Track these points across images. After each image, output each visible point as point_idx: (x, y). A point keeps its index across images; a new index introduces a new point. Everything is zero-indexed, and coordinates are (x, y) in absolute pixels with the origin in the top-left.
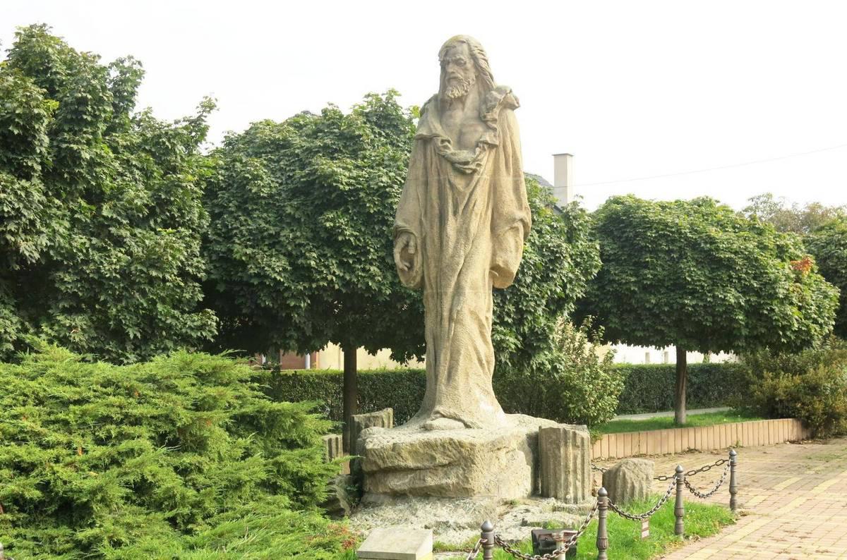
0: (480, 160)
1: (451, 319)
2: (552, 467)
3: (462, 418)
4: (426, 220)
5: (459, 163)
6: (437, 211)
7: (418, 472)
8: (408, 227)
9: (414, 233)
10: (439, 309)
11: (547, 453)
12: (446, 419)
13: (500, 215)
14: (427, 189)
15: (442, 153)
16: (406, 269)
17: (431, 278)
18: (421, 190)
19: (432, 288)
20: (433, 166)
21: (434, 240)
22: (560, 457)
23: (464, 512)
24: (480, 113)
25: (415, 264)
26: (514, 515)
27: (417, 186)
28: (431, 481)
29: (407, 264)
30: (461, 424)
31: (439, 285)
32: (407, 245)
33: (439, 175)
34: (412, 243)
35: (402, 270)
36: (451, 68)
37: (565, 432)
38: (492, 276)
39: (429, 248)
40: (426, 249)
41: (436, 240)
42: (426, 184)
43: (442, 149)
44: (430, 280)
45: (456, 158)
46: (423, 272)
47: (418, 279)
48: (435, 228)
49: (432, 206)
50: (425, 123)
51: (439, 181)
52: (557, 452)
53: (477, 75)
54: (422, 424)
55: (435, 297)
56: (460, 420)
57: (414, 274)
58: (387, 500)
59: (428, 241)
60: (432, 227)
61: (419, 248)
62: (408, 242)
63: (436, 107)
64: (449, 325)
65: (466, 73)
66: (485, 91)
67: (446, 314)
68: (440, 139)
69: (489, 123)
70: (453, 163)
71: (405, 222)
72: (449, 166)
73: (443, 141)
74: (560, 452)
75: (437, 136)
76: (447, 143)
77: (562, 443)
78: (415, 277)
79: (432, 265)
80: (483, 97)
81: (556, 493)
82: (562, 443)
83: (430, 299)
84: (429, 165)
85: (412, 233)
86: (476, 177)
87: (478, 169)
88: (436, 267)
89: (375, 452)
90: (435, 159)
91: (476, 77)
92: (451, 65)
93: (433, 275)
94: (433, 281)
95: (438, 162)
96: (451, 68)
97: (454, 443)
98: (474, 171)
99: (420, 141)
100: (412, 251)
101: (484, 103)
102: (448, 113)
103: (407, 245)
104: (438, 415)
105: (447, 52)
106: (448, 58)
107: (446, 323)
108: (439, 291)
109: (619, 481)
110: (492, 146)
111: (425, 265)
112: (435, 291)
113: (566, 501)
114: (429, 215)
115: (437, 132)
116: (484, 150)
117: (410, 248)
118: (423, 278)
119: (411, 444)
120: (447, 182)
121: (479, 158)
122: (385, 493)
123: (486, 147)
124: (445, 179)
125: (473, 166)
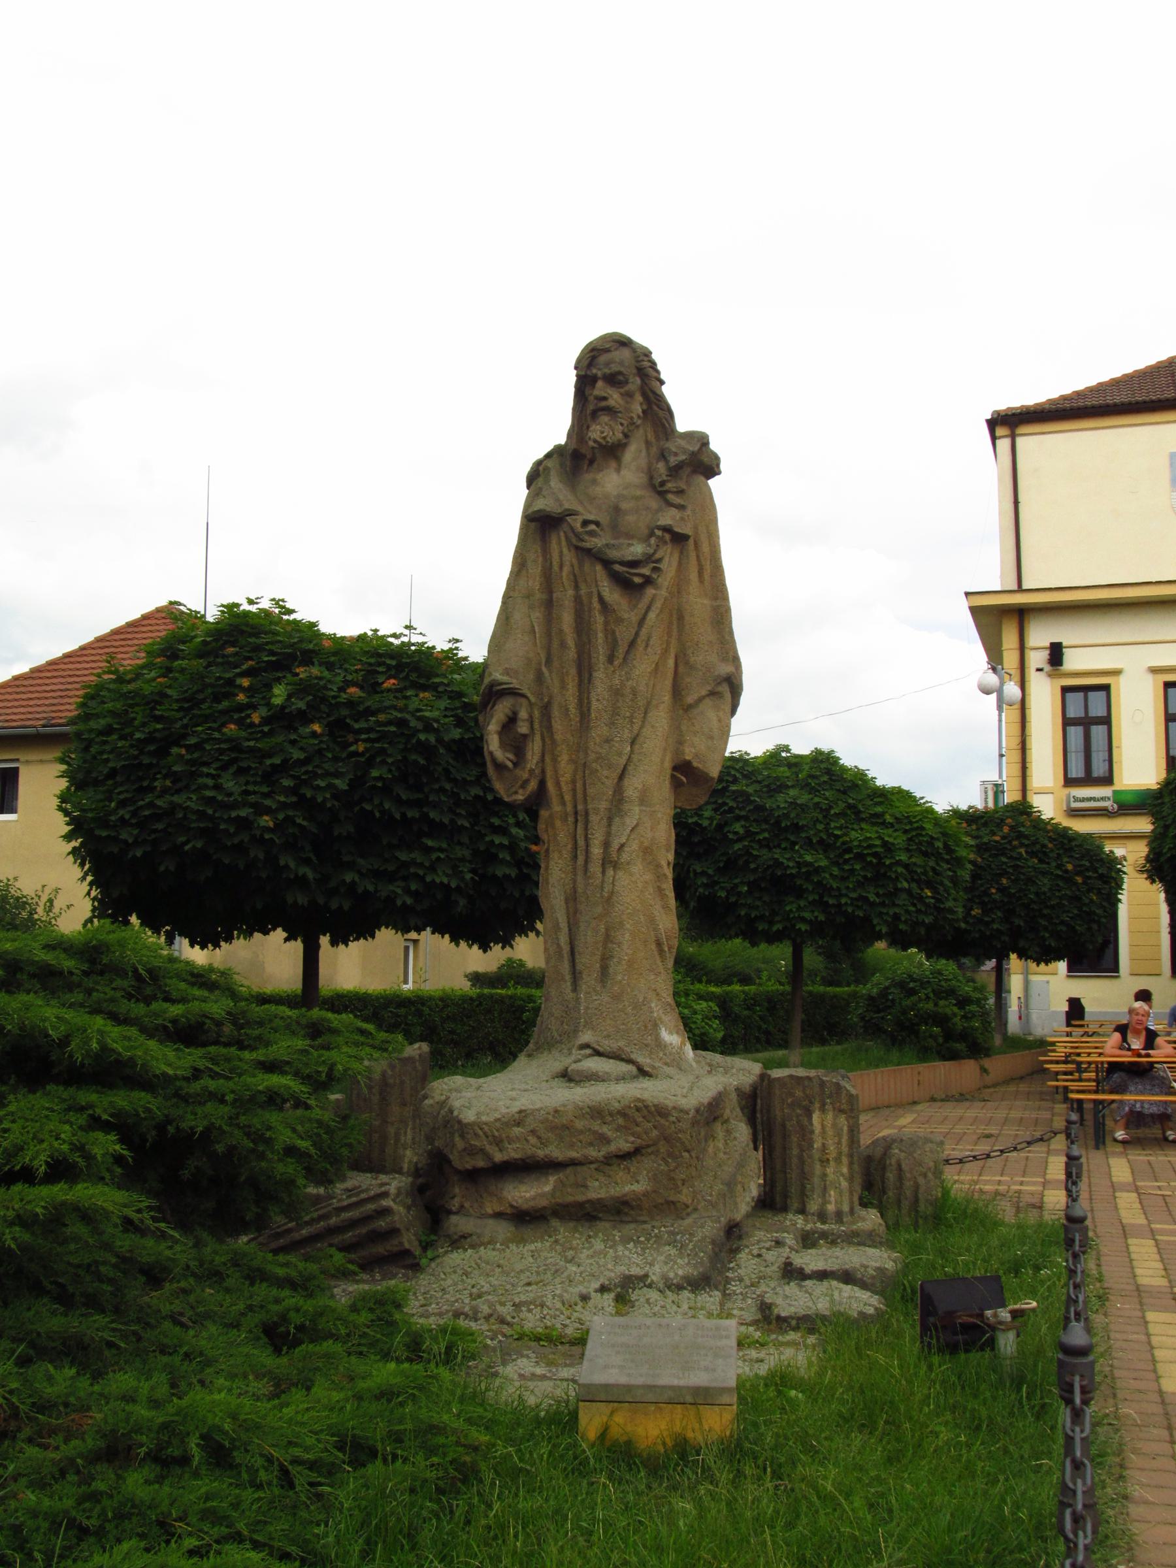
0: (659, 561)
1: (608, 862)
2: (795, 1152)
3: (633, 1056)
4: (550, 672)
5: (622, 563)
6: (572, 653)
7: (569, 1170)
8: (515, 684)
9: (529, 695)
10: (581, 842)
11: (784, 1126)
12: (604, 1059)
13: (691, 667)
14: (550, 614)
15: (584, 545)
16: (510, 765)
17: (563, 784)
18: (537, 615)
19: (563, 803)
20: (566, 569)
21: (567, 710)
22: (812, 1132)
23: (673, 1252)
24: (651, 478)
25: (529, 755)
26: (755, 1252)
27: (531, 607)
28: (598, 1189)
29: (511, 756)
30: (632, 1069)
31: (580, 795)
32: (512, 720)
33: (577, 587)
34: (523, 714)
35: (500, 767)
36: (600, 388)
37: (822, 1084)
38: (676, 785)
39: (558, 725)
40: (549, 728)
41: (573, 710)
42: (549, 604)
43: (586, 537)
44: (558, 784)
45: (614, 554)
46: (543, 772)
47: (533, 785)
48: (570, 686)
49: (563, 645)
50: (544, 493)
51: (578, 599)
52: (805, 1122)
53: (645, 407)
54: (558, 1066)
55: (571, 819)
56: (630, 1061)
57: (525, 776)
58: (503, 1229)
59: (556, 712)
60: (563, 686)
61: (536, 725)
62: (515, 714)
63: (562, 465)
64: (603, 872)
65: (627, 402)
66: (658, 438)
67: (597, 851)
68: (580, 519)
69: (670, 497)
70: (607, 563)
71: (508, 674)
72: (599, 568)
73: (586, 523)
74: (812, 1124)
75: (572, 513)
76: (593, 527)
77: (817, 1105)
78: (526, 782)
79: (564, 758)
80: (654, 450)
81: (803, 1204)
82: (817, 1105)
83: (558, 823)
84: (556, 568)
85: (523, 696)
86: (650, 591)
87: (655, 576)
88: (571, 761)
89: (481, 1129)
90: (569, 556)
91: (644, 412)
92: (600, 384)
93: (565, 778)
94: (564, 788)
95: (575, 561)
96: (600, 388)
97: (646, 1107)
98: (648, 581)
99: (533, 525)
100: (523, 728)
101: (658, 461)
102: (588, 477)
103: (512, 720)
104: (588, 1051)
105: (593, 358)
106: (594, 371)
107: (595, 868)
108: (580, 807)
109: (891, 1176)
110: (679, 539)
111: (548, 759)
112: (569, 808)
113: (822, 1216)
114: (556, 664)
115: (567, 506)
116: (665, 543)
117: (520, 723)
118: (542, 784)
119: (556, 1111)
120: (595, 600)
121: (657, 556)
122: (498, 1215)
123: (667, 537)
124: (590, 595)
125: (646, 571)
